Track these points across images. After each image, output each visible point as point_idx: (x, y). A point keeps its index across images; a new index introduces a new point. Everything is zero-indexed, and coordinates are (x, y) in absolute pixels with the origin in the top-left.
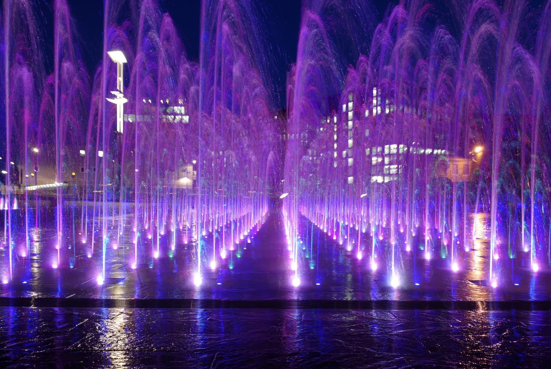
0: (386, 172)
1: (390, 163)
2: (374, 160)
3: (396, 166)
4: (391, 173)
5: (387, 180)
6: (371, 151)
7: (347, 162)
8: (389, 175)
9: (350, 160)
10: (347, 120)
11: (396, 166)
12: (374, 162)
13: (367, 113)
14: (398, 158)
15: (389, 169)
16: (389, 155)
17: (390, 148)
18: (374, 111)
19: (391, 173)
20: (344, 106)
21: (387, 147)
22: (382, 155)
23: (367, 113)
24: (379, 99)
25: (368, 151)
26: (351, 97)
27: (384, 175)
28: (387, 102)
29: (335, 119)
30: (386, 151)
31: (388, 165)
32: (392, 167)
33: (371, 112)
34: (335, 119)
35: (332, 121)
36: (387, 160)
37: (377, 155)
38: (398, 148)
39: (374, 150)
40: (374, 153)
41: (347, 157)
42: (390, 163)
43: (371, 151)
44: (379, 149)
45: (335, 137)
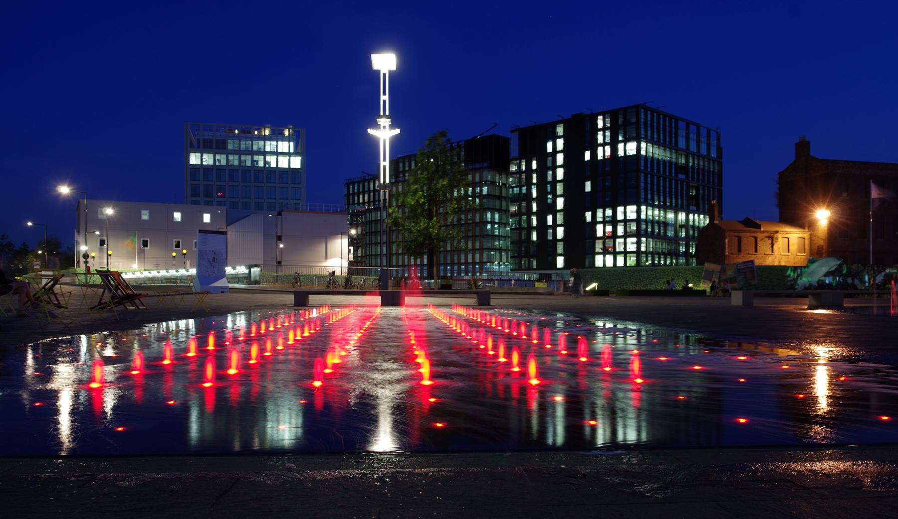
0: (620, 248)
1: (626, 236)
2: (599, 230)
3: (634, 240)
4: (628, 250)
5: (620, 262)
6: (594, 216)
7: (554, 234)
8: (625, 253)
9: (560, 232)
10: (554, 167)
11: (634, 240)
12: (600, 233)
13: (588, 156)
14: (638, 226)
15: (625, 244)
16: (625, 221)
17: (625, 213)
18: (600, 150)
19: (628, 250)
20: (550, 145)
21: (620, 209)
22: (614, 222)
23: (588, 156)
24: (608, 133)
25: (588, 216)
26: (560, 130)
27: (615, 254)
28: (620, 138)
29: (534, 165)
30: (620, 217)
31: (620, 237)
32: (629, 240)
33: (594, 155)
34: (534, 165)
35: (529, 165)
36: (620, 230)
37: (604, 223)
38: (639, 212)
39: (599, 214)
40: (599, 219)
41: (555, 225)
42: (626, 236)
43: (594, 216)
44: (609, 212)
45: (535, 194)
